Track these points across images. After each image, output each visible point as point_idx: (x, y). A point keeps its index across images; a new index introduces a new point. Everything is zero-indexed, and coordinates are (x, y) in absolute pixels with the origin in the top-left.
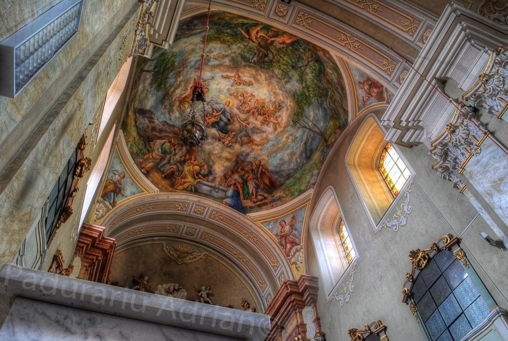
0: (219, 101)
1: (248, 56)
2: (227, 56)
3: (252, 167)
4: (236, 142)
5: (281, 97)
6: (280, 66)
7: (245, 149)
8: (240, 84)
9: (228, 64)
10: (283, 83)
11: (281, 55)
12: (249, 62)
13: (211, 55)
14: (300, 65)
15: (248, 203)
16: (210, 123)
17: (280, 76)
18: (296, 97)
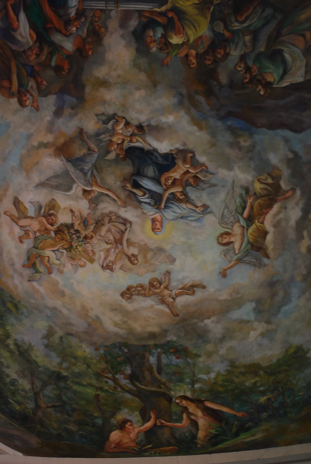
0: (181, 223)
1: (174, 360)
2: (223, 339)
3: (37, 83)
4: (98, 134)
5: (41, 290)
6: (89, 366)
8: (151, 284)
9: (207, 321)
10: (57, 329)
11: (103, 394)
12: (162, 346)
13: (261, 327)
14: (49, 388)
16: (179, 163)
17: (74, 341)
18: (9, 305)
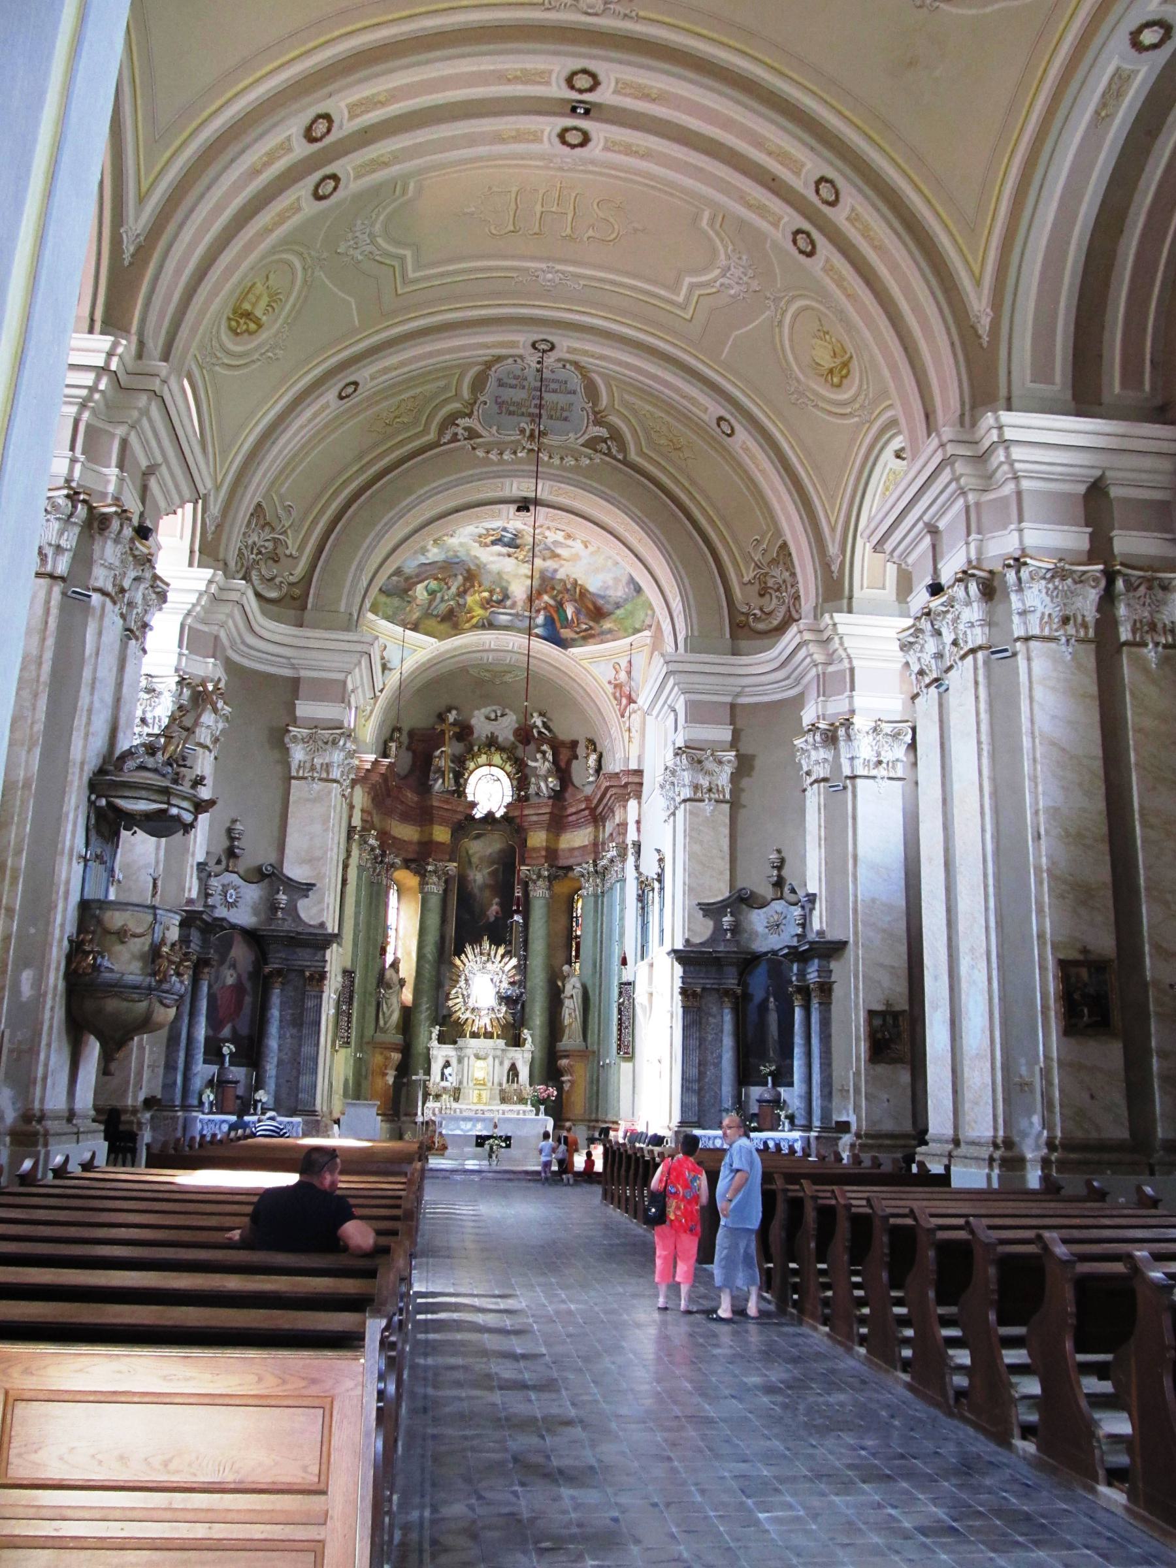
7: (550, 564)
15: (566, 633)
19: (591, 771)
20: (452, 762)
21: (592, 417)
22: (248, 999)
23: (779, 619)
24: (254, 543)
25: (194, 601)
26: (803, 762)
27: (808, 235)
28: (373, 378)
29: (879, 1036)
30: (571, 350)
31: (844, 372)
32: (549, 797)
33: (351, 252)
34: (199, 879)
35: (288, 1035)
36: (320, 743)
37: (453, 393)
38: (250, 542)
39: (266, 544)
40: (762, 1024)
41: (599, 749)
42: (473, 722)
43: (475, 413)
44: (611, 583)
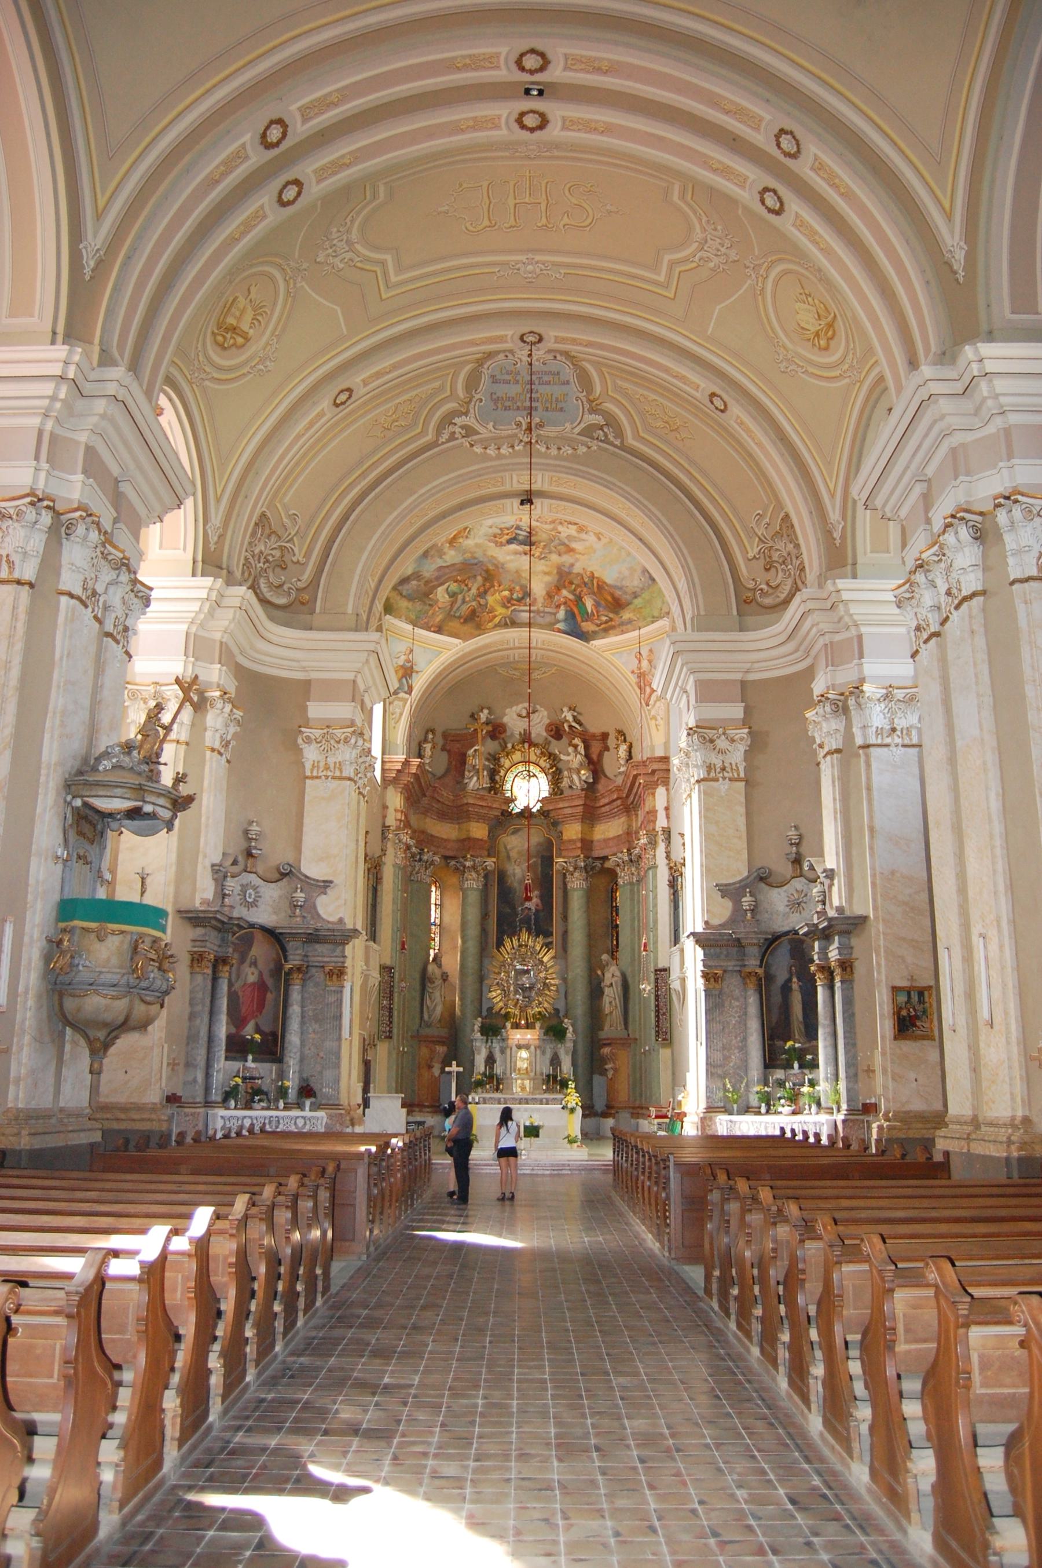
7: (567, 559)
15: (587, 626)
19: (622, 762)
20: (488, 760)
21: (587, 406)
22: (270, 997)
23: (786, 593)
24: (261, 552)
25: (197, 609)
26: (816, 735)
27: (775, 192)
28: (365, 383)
29: (904, 1013)
30: (557, 340)
31: (830, 333)
32: (582, 790)
33: (331, 260)
34: (215, 880)
35: (311, 1030)
36: (332, 742)
37: (448, 393)
38: (257, 551)
39: (273, 552)
40: (786, 1007)
41: (628, 739)
42: (506, 720)
43: (472, 411)
44: (627, 573)
